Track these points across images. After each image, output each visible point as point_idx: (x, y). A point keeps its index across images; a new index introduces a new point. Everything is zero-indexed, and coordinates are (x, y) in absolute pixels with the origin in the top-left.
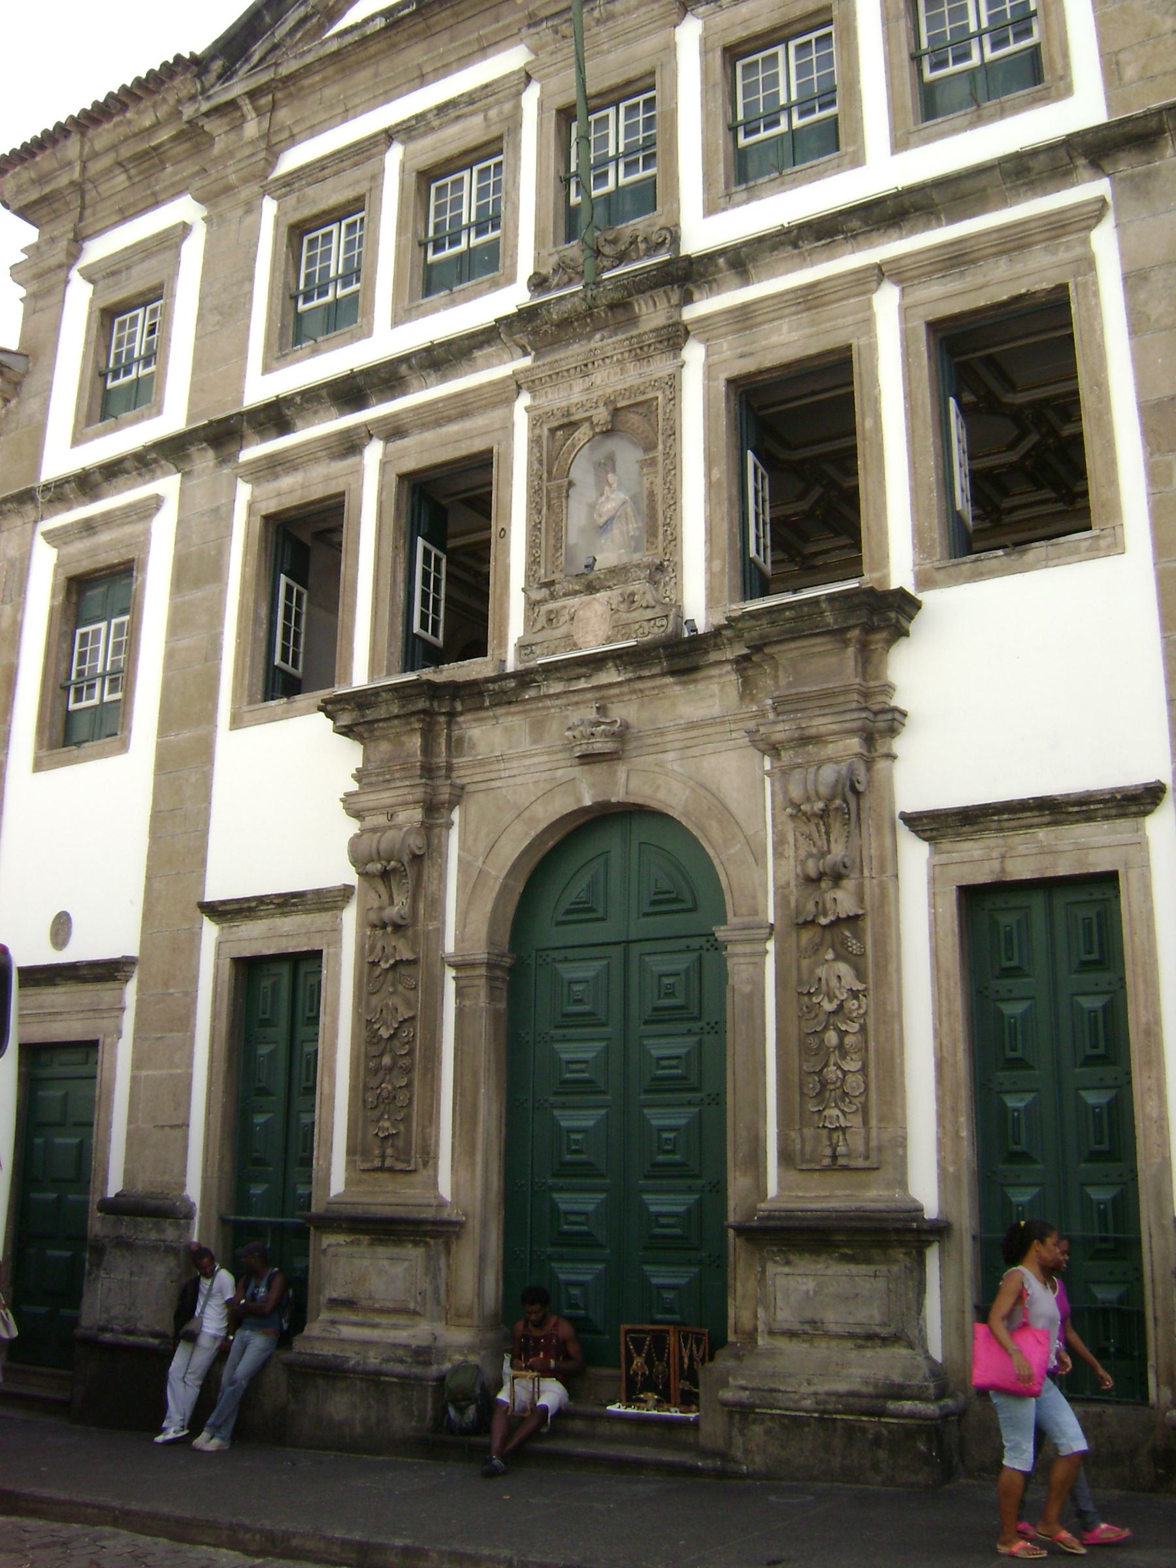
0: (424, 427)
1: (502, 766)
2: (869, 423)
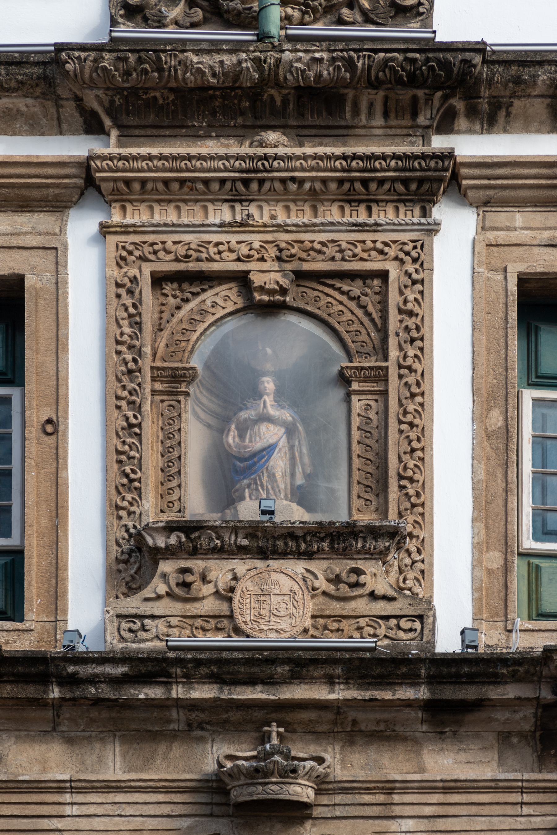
1: (68, 798)
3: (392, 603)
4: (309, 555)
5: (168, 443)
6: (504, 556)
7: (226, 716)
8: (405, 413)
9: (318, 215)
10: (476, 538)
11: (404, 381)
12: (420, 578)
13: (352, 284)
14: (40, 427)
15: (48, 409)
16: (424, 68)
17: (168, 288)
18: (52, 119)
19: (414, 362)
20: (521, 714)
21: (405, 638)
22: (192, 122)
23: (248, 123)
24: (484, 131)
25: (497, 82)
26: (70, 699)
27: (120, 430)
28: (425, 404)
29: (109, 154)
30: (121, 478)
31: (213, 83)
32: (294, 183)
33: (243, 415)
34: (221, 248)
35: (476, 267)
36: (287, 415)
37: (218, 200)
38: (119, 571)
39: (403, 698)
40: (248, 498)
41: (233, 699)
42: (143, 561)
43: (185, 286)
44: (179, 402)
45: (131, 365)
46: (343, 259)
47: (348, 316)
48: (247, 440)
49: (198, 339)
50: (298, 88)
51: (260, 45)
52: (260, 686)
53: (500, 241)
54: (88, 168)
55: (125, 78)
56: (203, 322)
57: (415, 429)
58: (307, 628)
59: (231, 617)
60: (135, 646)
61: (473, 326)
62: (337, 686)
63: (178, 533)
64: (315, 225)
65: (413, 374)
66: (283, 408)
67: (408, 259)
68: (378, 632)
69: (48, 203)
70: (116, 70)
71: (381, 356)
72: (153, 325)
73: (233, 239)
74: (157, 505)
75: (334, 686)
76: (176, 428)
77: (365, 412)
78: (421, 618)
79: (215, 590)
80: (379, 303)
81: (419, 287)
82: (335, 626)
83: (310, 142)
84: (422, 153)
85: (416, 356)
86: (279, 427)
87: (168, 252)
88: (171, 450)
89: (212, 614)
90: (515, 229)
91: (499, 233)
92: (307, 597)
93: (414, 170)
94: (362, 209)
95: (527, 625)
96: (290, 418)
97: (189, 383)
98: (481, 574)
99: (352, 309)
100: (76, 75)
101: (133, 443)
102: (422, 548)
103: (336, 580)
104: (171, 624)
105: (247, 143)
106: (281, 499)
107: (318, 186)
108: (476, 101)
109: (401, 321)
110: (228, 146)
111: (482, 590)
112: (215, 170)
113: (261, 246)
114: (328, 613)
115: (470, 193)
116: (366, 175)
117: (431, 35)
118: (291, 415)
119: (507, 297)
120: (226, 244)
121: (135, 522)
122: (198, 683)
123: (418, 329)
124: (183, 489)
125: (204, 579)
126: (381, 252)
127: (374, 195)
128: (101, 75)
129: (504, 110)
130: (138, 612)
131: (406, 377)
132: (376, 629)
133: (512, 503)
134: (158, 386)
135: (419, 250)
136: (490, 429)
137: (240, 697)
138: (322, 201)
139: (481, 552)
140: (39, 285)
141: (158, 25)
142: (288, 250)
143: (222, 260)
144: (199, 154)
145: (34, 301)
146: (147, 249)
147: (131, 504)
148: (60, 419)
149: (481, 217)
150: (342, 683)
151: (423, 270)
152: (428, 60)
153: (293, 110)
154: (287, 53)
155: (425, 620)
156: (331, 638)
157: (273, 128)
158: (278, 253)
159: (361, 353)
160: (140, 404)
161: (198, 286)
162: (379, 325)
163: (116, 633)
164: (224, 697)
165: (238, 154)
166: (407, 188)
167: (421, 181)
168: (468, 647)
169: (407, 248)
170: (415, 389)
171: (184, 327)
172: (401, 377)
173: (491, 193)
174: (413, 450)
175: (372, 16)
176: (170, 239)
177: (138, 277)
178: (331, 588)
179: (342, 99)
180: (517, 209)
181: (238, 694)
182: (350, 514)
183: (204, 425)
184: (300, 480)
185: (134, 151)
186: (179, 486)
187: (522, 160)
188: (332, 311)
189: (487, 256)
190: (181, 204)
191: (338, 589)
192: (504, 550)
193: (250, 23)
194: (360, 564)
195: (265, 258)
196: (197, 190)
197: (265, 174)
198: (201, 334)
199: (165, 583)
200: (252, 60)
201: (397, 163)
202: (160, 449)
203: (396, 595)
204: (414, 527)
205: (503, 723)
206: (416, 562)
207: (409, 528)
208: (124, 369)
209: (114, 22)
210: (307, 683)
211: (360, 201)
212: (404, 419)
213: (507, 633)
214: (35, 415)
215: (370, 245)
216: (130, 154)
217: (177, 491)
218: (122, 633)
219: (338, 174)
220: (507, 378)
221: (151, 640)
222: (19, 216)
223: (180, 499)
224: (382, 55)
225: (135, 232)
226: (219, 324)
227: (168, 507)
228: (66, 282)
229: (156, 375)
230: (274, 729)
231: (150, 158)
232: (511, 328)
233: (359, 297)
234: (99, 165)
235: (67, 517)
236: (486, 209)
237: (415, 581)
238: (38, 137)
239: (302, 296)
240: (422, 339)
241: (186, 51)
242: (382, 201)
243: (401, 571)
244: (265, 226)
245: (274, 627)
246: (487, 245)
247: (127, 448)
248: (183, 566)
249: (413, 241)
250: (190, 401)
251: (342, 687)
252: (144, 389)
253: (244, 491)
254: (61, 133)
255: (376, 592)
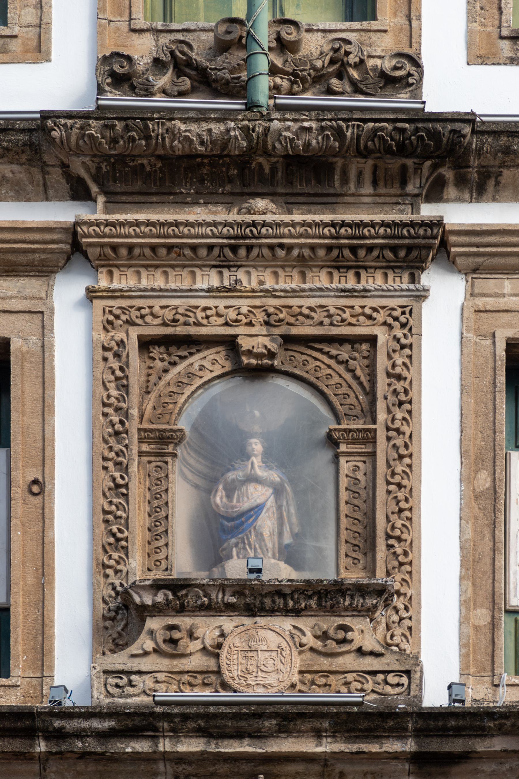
3: (379, 659)
4: (297, 612)
5: (156, 503)
6: (491, 613)
7: (214, 768)
8: (393, 474)
9: (307, 281)
10: (464, 596)
11: (392, 443)
12: (408, 634)
13: (341, 348)
14: (26, 487)
15: (34, 470)
16: (413, 137)
17: (155, 352)
18: (38, 185)
19: (402, 424)
20: (507, 766)
21: (392, 693)
22: (180, 189)
23: (236, 191)
24: (474, 200)
25: (487, 152)
26: (56, 753)
27: (106, 490)
28: (413, 466)
29: (96, 220)
30: (108, 537)
31: (201, 150)
32: (283, 250)
33: (231, 476)
34: (209, 312)
35: (464, 332)
36: (275, 475)
37: (205, 266)
38: (106, 628)
39: (390, 750)
40: (235, 557)
41: (220, 752)
42: (130, 618)
43: (173, 349)
44: (166, 463)
45: (119, 427)
46: (332, 324)
47: (336, 379)
48: (235, 501)
49: (186, 401)
50: (286, 156)
51: (249, 114)
52: (247, 739)
53: (489, 308)
54: (75, 233)
55: (112, 145)
56: (191, 385)
57: (403, 489)
58: (295, 683)
59: (218, 672)
60: (121, 701)
61: (462, 389)
62: (324, 739)
63: (165, 591)
64: (303, 290)
65: (401, 436)
66: (271, 469)
67: (396, 324)
68: (366, 687)
69: (34, 268)
70: (102, 138)
71: (369, 419)
72: (140, 388)
73: (221, 303)
74: (144, 564)
75: (322, 739)
76: (163, 488)
77: (353, 473)
78: (408, 673)
79: (202, 646)
80: (367, 367)
81: (407, 351)
82: (323, 681)
83: (298, 209)
84: (411, 221)
85: (404, 419)
86: (266, 488)
87: (155, 316)
88: (158, 510)
89: (199, 670)
90: (504, 296)
91: (487, 299)
92: (295, 653)
93: (403, 237)
94: (351, 275)
95: (514, 680)
96: (278, 479)
97: (176, 445)
98: (469, 630)
99: (341, 373)
100: (62, 143)
101: (120, 503)
102: (409, 606)
103: (324, 636)
104: (158, 679)
105: (235, 210)
106: (269, 558)
107: (306, 252)
108: (465, 170)
109: (389, 385)
110: (216, 213)
111: (469, 646)
112: (203, 237)
113: (249, 311)
114: (315, 668)
115: (459, 260)
116: (355, 242)
117: (420, 106)
118: (279, 476)
119: (495, 361)
120: (214, 309)
121: (122, 580)
122: (185, 737)
123: (406, 392)
124: (170, 548)
125: (191, 636)
126: (370, 317)
127: (362, 262)
128: (88, 142)
129: (493, 179)
130: (125, 668)
131: (394, 439)
132: (363, 684)
133: (500, 562)
134: (145, 447)
135: (407, 316)
136: (478, 490)
137: (227, 750)
138: (310, 267)
139: (468, 609)
140: (24, 349)
141: (145, 93)
142: (277, 314)
143: (210, 324)
144: (187, 221)
145: (20, 364)
146: (134, 313)
147: (118, 563)
148: (46, 480)
149: (469, 283)
150: (330, 736)
151: (412, 335)
152: (417, 130)
153: (282, 178)
154: (276, 122)
155: (412, 676)
156: (318, 693)
157: (261, 195)
158: (266, 318)
159: (349, 415)
160: (127, 465)
161: (185, 350)
162: (368, 389)
163: (103, 689)
164: (211, 750)
165: (226, 221)
166: (396, 255)
167: (410, 248)
168: (455, 701)
169: (395, 314)
170: (403, 451)
171: (171, 389)
172: (389, 439)
173: (480, 260)
174: (401, 510)
175: (361, 86)
176: (157, 303)
177: (125, 340)
178: (318, 644)
179: (330, 168)
180: (505, 276)
181: (225, 747)
182: (338, 573)
183: (192, 486)
184: (287, 540)
185: (121, 217)
186: (167, 545)
187: (511, 228)
188: (320, 375)
189: (476, 321)
190: (169, 270)
191: (326, 646)
192: (491, 607)
193: (239, 92)
194: (348, 621)
195: (253, 322)
196: (184, 255)
197: (253, 241)
198: (189, 397)
199: (152, 639)
200: (240, 129)
201: (386, 230)
202: (148, 509)
203: (383, 651)
204: (402, 585)
205: (490, 775)
206: (404, 619)
207: (397, 586)
208: (110, 430)
209: (100, 91)
210: (294, 737)
211: (349, 268)
212: (392, 480)
213: (494, 688)
214: (20, 476)
215: (358, 310)
216: (117, 220)
217: (164, 550)
218: (109, 688)
219: (327, 241)
220: (495, 440)
221: (138, 695)
222: (4, 280)
223: (167, 558)
224: (371, 125)
225: (122, 297)
226: (206, 386)
227: (155, 565)
228: (53, 346)
229: (143, 437)
231: (138, 224)
232: (499, 391)
233: (347, 361)
234: (86, 230)
235: (52, 575)
236: (475, 276)
237: (403, 638)
238: (23, 203)
239: (290, 360)
240: (410, 402)
241: (173, 119)
242: (371, 267)
243: (388, 628)
244: (253, 291)
245: (262, 683)
246: (475, 311)
247: (113, 508)
248: (170, 623)
249: (401, 307)
250: (177, 462)
251: (329, 740)
252: (131, 450)
253: (232, 550)
254: (47, 199)
255: (364, 648)
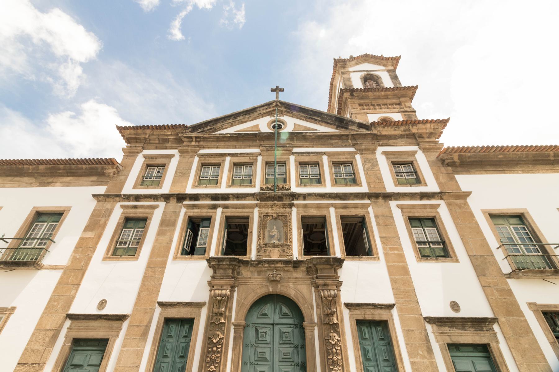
0: (233, 208)
2: (330, 229)
4: (279, 248)
125: (267, 251)
230: (275, 270)
